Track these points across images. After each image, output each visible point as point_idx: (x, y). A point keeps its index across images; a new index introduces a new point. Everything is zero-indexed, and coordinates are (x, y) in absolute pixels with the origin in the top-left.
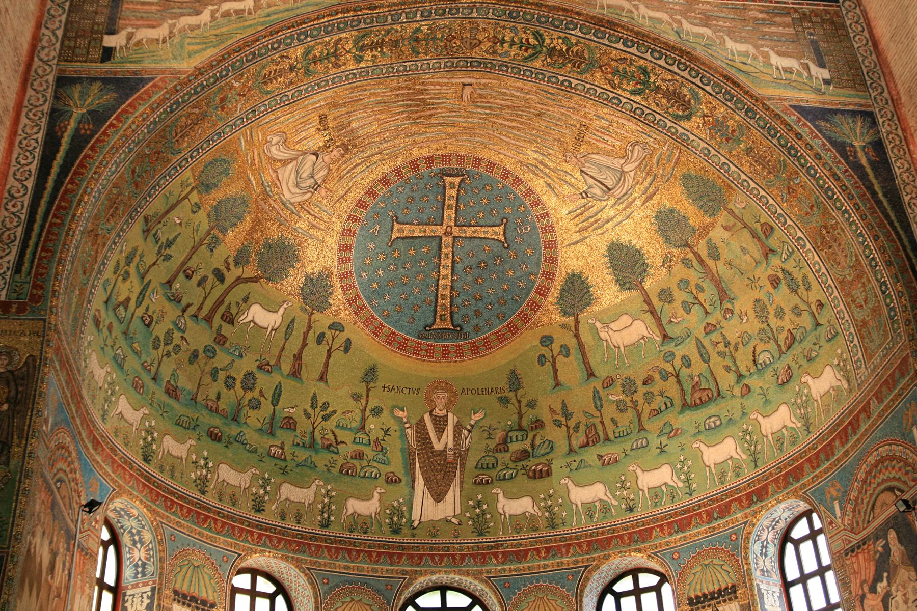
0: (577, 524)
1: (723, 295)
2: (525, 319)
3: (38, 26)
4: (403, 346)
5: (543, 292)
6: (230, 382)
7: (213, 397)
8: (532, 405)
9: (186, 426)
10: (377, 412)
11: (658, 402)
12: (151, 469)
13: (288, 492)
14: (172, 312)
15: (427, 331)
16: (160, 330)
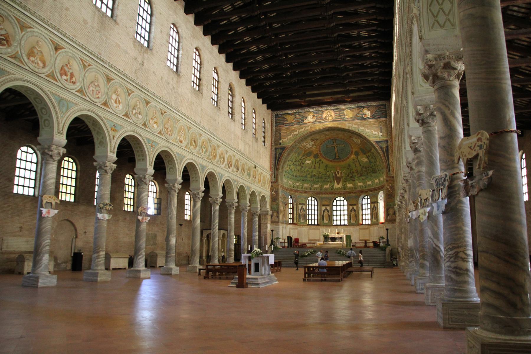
0: (359, 189)
1: (376, 159)
2: (350, 156)
3: (271, 140)
4: (331, 161)
5: (352, 153)
6: (305, 172)
7: (302, 174)
8: (352, 169)
9: (298, 180)
10: (328, 171)
11: (370, 171)
12: (295, 188)
13: (315, 186)
14: (294, 167)
15: (335, 159)
16: (293, 170)
